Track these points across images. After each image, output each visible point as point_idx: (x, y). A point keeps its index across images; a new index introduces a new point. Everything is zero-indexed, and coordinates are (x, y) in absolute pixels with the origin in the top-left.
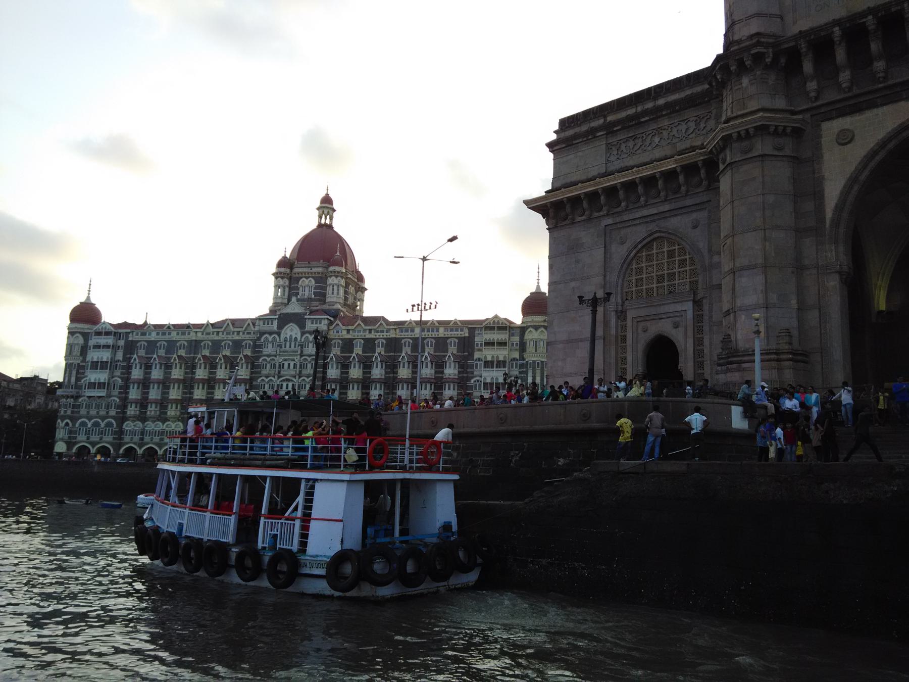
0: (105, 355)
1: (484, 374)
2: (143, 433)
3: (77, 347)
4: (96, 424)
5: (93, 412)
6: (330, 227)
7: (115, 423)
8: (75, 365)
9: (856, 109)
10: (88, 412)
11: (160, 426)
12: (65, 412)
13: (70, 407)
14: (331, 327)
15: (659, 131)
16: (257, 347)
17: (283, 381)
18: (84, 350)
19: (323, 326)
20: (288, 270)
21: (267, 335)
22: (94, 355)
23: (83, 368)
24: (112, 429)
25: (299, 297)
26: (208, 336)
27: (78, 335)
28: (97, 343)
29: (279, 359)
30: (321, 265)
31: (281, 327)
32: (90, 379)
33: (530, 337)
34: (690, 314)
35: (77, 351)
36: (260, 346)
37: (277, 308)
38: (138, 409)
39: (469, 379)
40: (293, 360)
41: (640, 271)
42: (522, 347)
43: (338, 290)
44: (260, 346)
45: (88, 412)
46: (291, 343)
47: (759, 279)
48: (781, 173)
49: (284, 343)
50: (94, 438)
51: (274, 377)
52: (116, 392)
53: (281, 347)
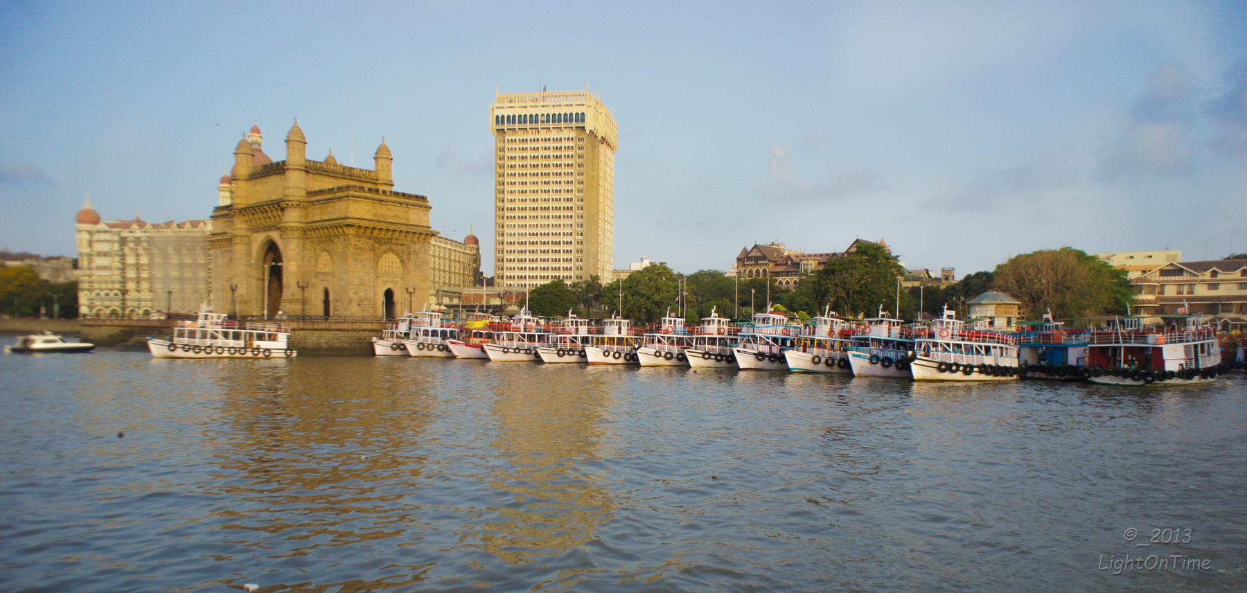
0: (105, 247)
4: (107, 294)
5: (103, 286)
18: (90, 243)
20: (228, 185)
22: (98, 247)
35: (85, 244)
50: (107, 303)
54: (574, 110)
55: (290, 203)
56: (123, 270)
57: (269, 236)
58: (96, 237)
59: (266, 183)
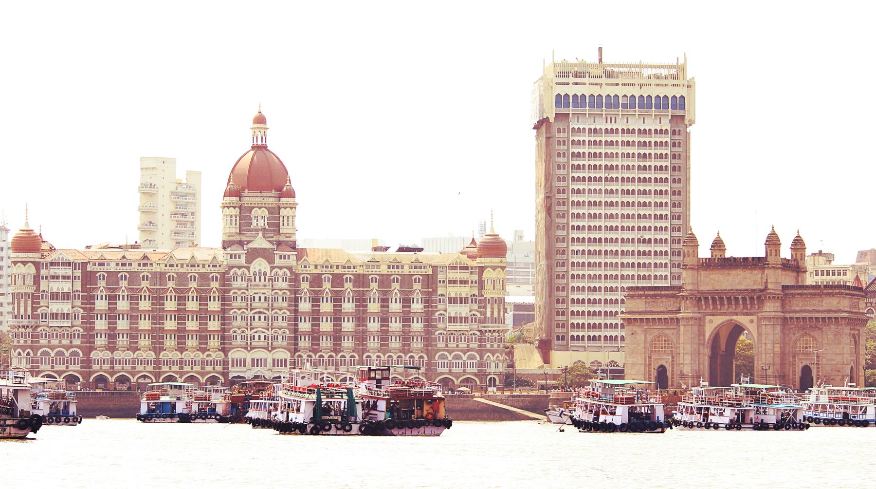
0: (66, 286)
1: (449, 309)
2: (112, 362)
3: (29, 276)
4: (60, 354)
5: (55, 342)
6: (264, 148)
7: (80, 352)
8: (22, 294)
9: (713, 315)
10: (49, 342)
11: (130, 355)
12: (18, 342)
13: (29, 337)
14: (299, 263)
15: (662, 302)
16: (225, 279)
17: (256, 313)
18: (37, 279)
19: (292, 261)
20: (235, 199)
21: (235, 269)
23: (38, 297)
24: (78, 359)
25: (252, 227)
26: (171, 268)
27: (30, 264)
28: (55, 273)
29: (251, 292)
30: (273, 195)
31: (249, 260)
32: (51, 309)
33: (489, 276)
34: (671, 360)
35: (30, 281)
36: (229, 280)
37: (231, 239)
38: (107, 339)
39: (433, 313)
40: (264, 294)
41: (655, 344)
42: (481, 285)
43: (288, 221)
44: (229, 280)
45: (49, 342)
46: (260, 278)
47: (690, 357)
48: (696, 328)
49: (253, 277)
50: (58, 367)
51: (247, 309)
52: (78, 322)
53: (251, 281)
54: (670, 92)
55: (777, 296)
56: (89, 317)
57: (731, 320)
58: (54, 271)
59: (729, 274)
